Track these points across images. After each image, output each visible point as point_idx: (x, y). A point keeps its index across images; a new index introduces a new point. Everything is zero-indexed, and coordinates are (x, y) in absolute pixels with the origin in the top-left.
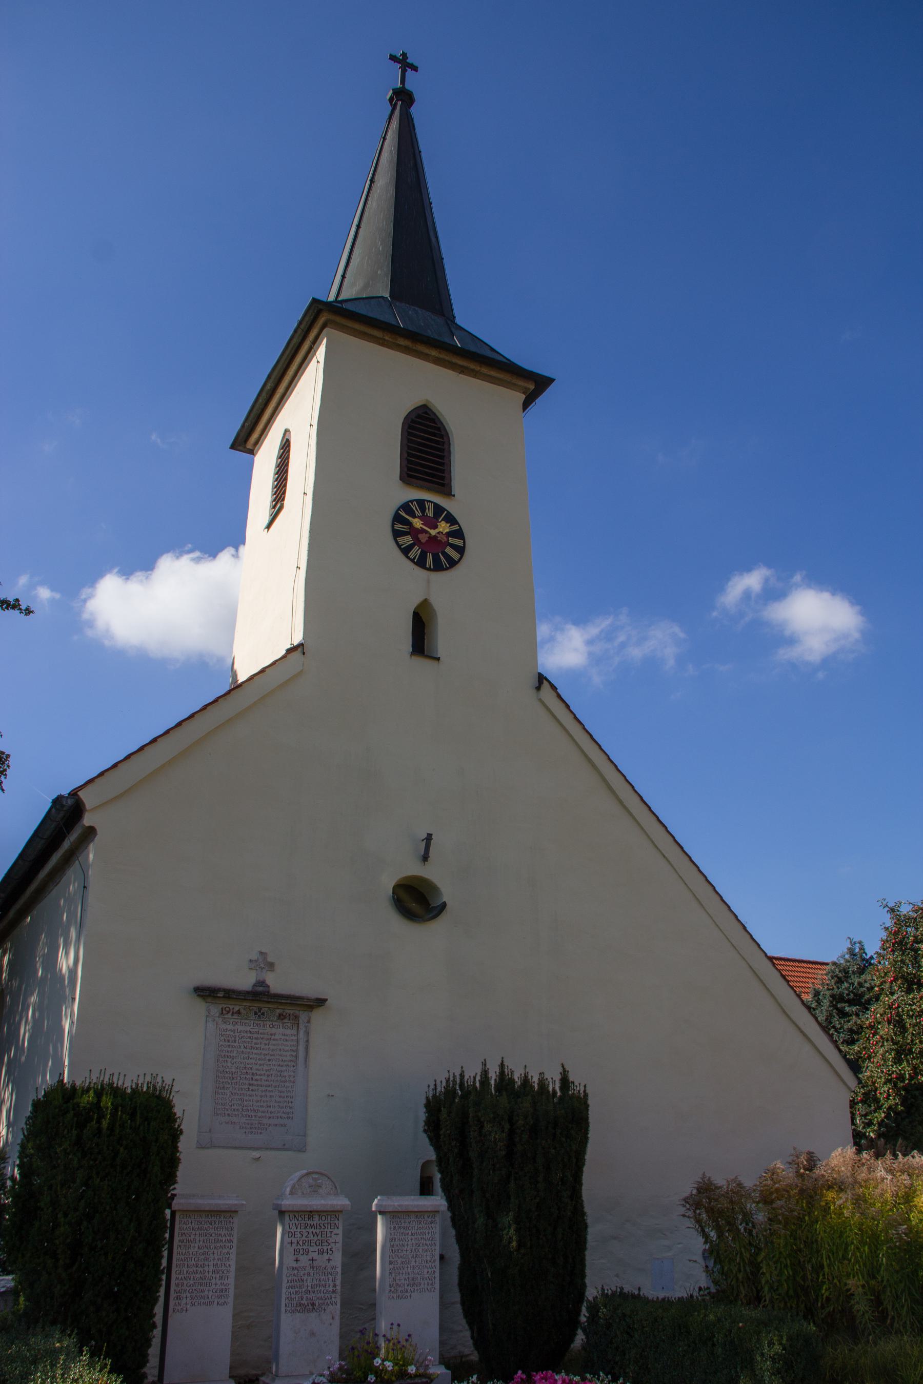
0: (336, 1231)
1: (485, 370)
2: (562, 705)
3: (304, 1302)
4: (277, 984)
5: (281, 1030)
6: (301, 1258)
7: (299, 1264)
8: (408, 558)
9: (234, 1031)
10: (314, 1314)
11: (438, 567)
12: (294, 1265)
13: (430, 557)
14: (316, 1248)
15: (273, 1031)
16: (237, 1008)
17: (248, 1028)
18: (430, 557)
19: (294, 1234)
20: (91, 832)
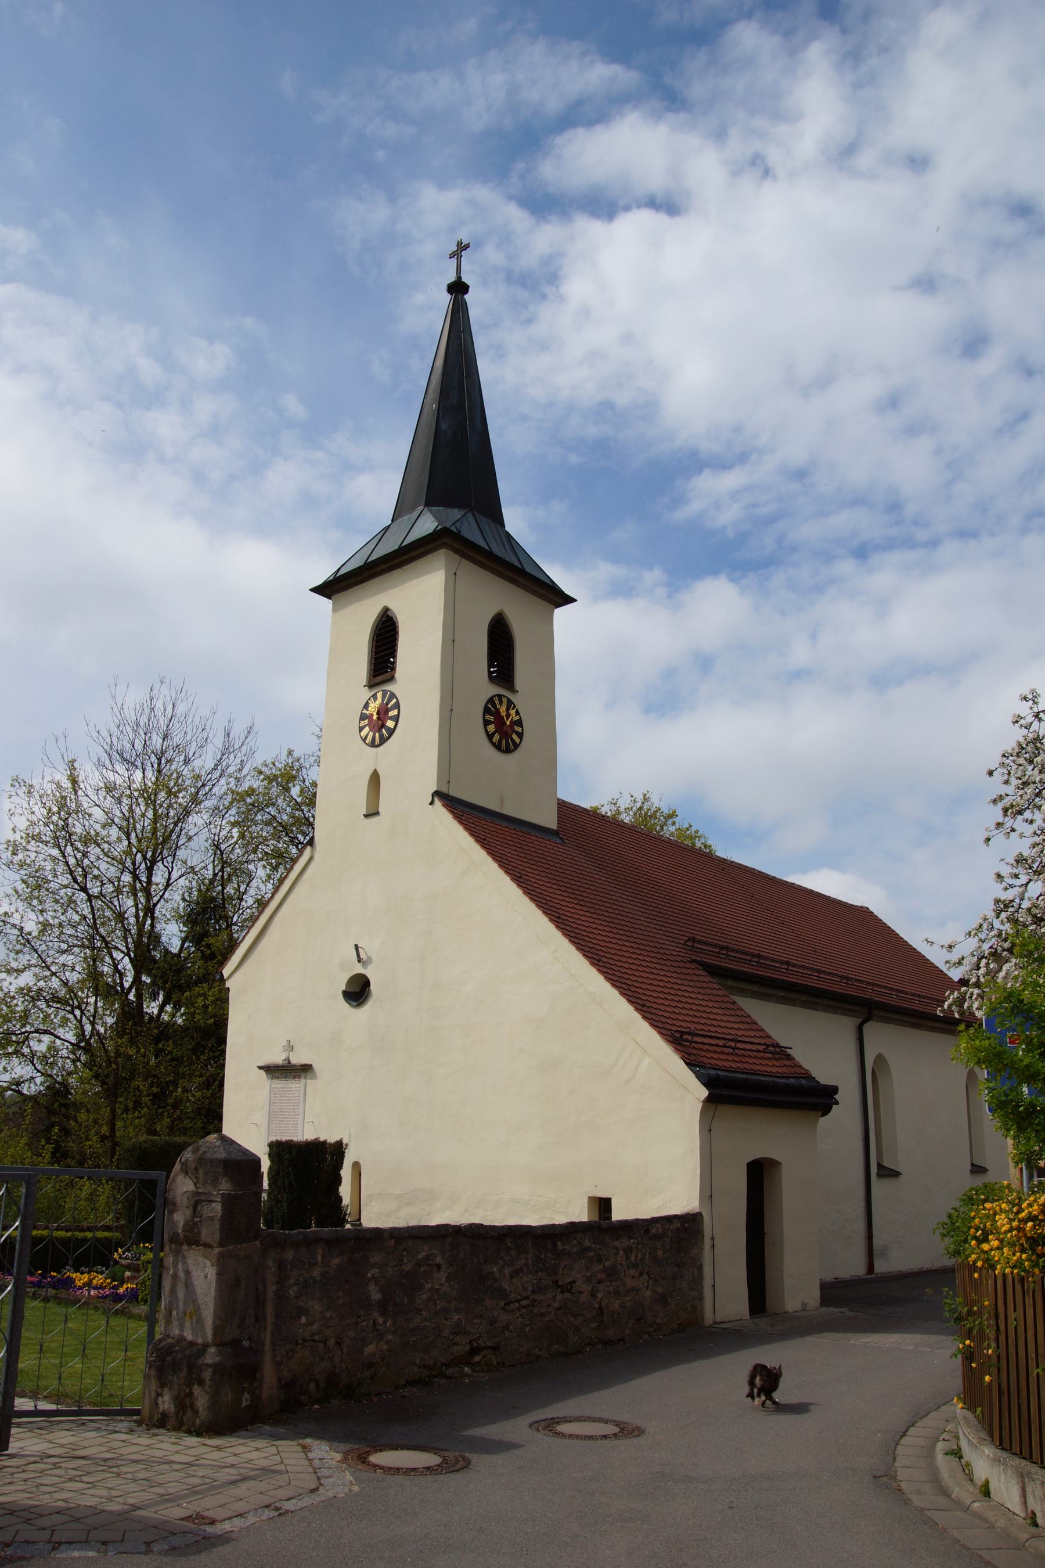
1: (414, 554)
5: (295, 1085)
15: (292, 1086)
17: (282, 1086)
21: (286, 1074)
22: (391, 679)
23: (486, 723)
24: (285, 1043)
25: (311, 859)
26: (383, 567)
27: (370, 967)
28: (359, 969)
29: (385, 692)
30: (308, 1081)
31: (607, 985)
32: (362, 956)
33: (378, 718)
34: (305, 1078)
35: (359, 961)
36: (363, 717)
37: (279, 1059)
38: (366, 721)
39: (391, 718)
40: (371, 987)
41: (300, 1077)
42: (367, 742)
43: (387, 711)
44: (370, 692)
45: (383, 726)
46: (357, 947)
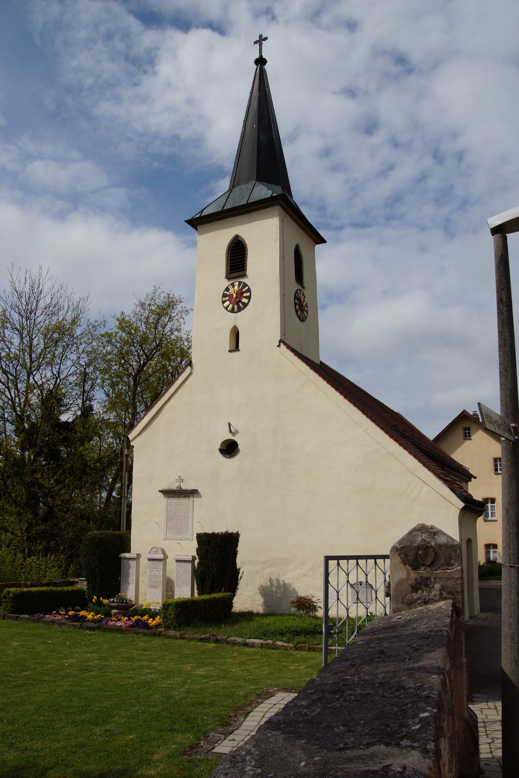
0: (161, 565)
1: (257, 207)
4: (184, 487)
5: (185, 501)
6: (152, 572)
8: (228, 311)
10: (155, 589)
14: (155, 570)
15: (183, 501)
17: (176, 502)
19: (150, 565)
20: (133, 447)
21: (179, 495)
22: (244, 275)
23: (295, 304)
24: (177, 477)
25: (191, 374)
26: (236, 212)
27: (237, 436)
28: (230, 437)
29: (240, 283)
30: (195, 499)
31: (401, 449)
33: (236, 297)
34: (193, 497)
35: (231, 432)
36: (224, 295)
37: (174, 486)
38: (227, 298)
39: (246, 297)
40: (239, 446)
41: (189, 497)
42: (229, 309)
43: (242, 293)
44: (229, 282)
45: (240, 301)
46: (229, 424)
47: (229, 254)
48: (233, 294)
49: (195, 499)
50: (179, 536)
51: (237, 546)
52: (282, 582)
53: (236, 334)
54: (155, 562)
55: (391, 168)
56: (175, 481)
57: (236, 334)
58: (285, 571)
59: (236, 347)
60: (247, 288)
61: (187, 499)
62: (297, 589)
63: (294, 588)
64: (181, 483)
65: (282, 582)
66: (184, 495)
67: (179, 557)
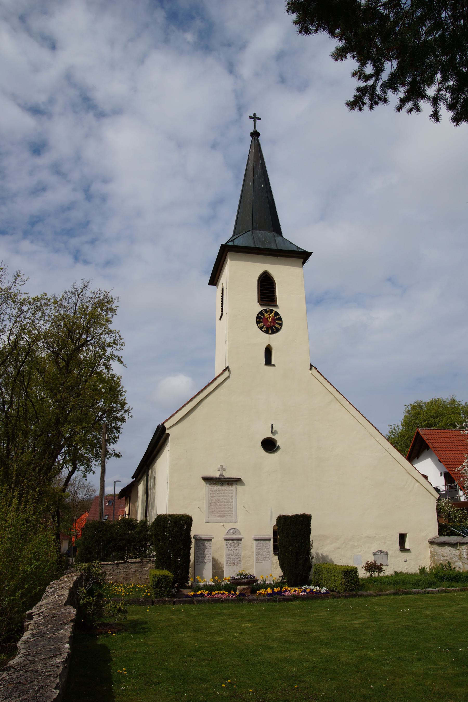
2: (319, 374)
3: (232, 563)
5: (228, 488)
7: (230, 553)
9: (214, 489)
10: (235, 566)
11: (273, 332)
12: (229, 553)
13: (270, 329)
14: (234, 549)
15: (226, 488)
16: (214, 482)
17: (218, 488)
18: (270, 329)
25: (228, 377)
28: (270, 435)
32: (273, 431)
35: (272, 432)
36: (258, 317)
37: (217, 475)
38: (261, 320)
41: (232, 484)
42: (263, 329)
47: (259, 284)
48: (268, 318)
49: (239, 486)
50: (223, 519)
51: (310, 526)
52: (321, 555)
53: (268, 351)
54: (234, 542)
55: (44, 189)
56: (217, 470)
57: (268, 351)
58: (322, 546)
59: (268, 361)
60: (279, 316)
61: (230, 486)
62: (333, 560)
63: (331, 559)
64: (224, 472)
65: (321, 555)
66: (227, 483)
67: (256, 536)
